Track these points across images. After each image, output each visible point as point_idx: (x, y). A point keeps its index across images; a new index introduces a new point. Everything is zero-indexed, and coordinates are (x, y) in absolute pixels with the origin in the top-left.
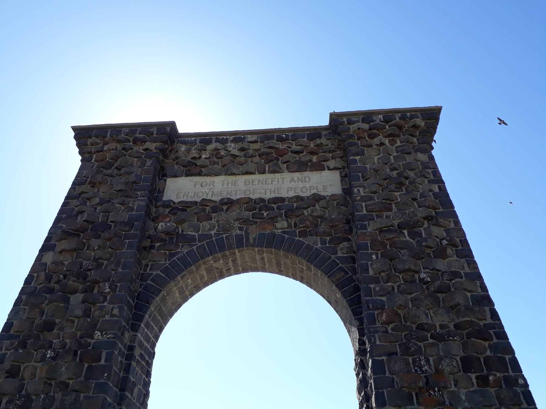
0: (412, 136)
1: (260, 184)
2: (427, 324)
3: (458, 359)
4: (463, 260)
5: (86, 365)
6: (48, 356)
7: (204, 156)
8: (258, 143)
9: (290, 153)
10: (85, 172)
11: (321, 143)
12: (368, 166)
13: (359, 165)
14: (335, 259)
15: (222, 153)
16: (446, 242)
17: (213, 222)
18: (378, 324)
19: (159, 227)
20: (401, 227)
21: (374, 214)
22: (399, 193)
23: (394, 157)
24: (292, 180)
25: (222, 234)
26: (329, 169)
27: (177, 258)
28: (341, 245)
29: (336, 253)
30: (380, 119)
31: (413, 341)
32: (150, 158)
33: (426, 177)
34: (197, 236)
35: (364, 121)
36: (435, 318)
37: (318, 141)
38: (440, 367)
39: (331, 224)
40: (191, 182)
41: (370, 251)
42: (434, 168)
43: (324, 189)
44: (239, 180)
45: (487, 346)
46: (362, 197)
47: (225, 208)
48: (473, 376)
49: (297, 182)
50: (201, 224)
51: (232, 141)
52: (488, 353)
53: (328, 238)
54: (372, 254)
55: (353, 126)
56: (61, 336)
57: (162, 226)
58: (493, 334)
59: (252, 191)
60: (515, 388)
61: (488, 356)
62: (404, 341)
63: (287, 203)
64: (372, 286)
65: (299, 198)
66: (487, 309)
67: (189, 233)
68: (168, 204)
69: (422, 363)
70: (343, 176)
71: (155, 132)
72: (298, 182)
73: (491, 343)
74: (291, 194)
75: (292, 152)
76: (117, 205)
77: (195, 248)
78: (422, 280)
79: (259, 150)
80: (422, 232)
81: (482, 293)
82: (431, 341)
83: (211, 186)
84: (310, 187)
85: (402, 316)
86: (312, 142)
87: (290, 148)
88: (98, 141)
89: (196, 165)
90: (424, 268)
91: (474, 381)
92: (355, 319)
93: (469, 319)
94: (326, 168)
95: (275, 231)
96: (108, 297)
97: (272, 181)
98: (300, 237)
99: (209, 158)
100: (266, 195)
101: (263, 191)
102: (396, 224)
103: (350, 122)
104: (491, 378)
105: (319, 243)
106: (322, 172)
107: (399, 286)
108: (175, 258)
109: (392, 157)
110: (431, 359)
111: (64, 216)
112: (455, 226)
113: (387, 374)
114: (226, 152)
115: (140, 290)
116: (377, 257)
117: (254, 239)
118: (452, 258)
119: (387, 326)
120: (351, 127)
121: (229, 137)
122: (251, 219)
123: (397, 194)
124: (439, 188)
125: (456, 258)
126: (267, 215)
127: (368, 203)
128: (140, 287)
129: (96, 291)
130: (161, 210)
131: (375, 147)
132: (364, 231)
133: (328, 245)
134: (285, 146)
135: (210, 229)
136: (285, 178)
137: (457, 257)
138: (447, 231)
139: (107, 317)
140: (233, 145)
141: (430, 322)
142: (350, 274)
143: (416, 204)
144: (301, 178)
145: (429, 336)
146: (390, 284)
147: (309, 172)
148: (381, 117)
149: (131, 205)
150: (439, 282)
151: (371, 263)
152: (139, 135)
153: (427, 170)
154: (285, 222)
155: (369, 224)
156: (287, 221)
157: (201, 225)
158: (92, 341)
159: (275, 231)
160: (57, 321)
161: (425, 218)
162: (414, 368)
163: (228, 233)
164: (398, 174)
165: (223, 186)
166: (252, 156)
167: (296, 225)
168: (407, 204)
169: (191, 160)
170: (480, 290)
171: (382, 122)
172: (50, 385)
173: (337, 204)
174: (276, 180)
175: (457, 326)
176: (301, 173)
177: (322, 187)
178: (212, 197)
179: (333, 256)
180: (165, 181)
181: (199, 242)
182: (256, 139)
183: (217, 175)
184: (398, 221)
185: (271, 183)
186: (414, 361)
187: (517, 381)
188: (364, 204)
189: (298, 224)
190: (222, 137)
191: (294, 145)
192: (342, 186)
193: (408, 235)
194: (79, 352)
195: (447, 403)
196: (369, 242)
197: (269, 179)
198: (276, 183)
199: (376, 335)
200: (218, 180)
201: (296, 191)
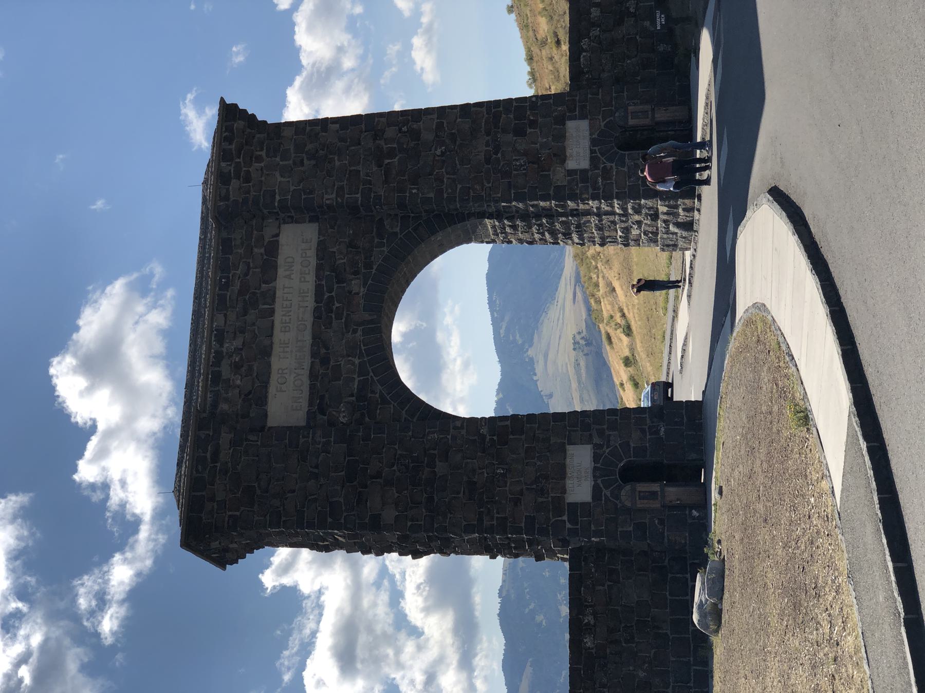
0: (254, 137)
1: (290, 314)
3: (515, 138)
4: (424, 118)
5: (511, 437)
7: (238, 382)
8: (228, 314)
9: (248, 277)
10: (256, 518)
11: (241, 238)
12: (292, 188)
13: (289, 197)
14: (402, 235)
15: (237, 360)
16: (406, 127)
17: (342, 363)
18: (483, 194)
19: (344, 420)
20: (380, 166)
21: (361, 187)
22: (336, 161)
23: (281, 161)
24: (289, 277)
25: (361, 350)
26: (278, 235)
27: (388, 394)
28: (388, 227)
29: (396, 234)
30: (227, 165)
31: (499, 168)
33: (318, 134)
34: (359, 379)
38: (522, 151)
40: (275, 397)
41: (408, 195)
42: (306, 124)
43: (307, 242)
44: (281, 340)
45: (505, 116)
46: (337, 196)
47: (323, 351)
48: (529, 130)
49: (293, 272)
50: (344, 376)
51: (222, 345)
52: (512, 116)
53: (376, 240)
54: (411, 193)
55: (231, 196)
56: (480, 471)
57: (344, 417)
58: (496, 110)
60: (539, 104)
61: (514, 117)
62: (499, 175)
63: (324, 283)
64: (445, 197)
65: (319, 268)
66: (473, 109)
67: (356, 386)
68: (310, 415)
69: (518, 164)
72: (293, 270)
73: (503, 112)
74: (311, 278)
75: (246, 274)
76: (320, 459)
77: (375, 379)
78: (443, 154)
79: (237, 312)
80: (389, 147)
82: (499, 155)
83: (284, 372)
84: (302, 257)
85: (476, 174)
87: (239, 278)
89: (250, 393)
90: (431, 151)
91: (532, 130)
92: (468, 221)
93: (483, 124)
94: (275, 239)
95: (361, 294)
96: (441, 436)
97: (286, 300)
100: (307, 307)
101: (301, 309)
102: (376, 168)
103: (226, 198)
104: (532, 118)
105: (382, 249)
106: (280, 244)
107: (447, 174)
108: (388, 397)
110: (514, 158)
111: (329, 520)
112: (385, 117)
113: (526, 191)
114: (234, 355)
116: (414, 188)
118: (421, 126)
119: (485, 187)
120: (232, 198)
121: (212, 350)
122: (343, 320)
123: (337, 163)
125: (421, 123)
126: (340, 303)
127: (346, 191)
129: (432, 452)
131: (263, 178)
132: (383, 197)
133: (385, 241)
134: (238, 284)
135: (353, 364)
136: (284, 285)
139: (464, 432)
141: (483, 154)
142: (421, 221)
143: (353, 148)
144: (287, 267)
145: (495, 156)
146: (445, 180)
147: (279, 257)
148: (223, 164)
149: (320, 446)
150: (447, 141)
151: (420, 194)
152: (208, 453)
153: (307, 130)
154: (353, 282)
155: (374, 192)
156: (352, 280)
157: (345, 376)
158: (488, 437)
159: (361, 294)
160: (465, 479)
161: (375, 139)
162: (521, 171)
163: (360, 344)
164: (309, 159)
165: (288, 358)
166: (245, 323)
167: (356, 273)
169: (241, 399)
170: (455, 111)
171: (231, 164)
172: (527, 463)
173: (332, 227)
175: (488, 134)
176: (278, 267)
177: (304, 244)
178: (303, 369)
179: (399, 237)
180: (270, 428)
182: (222, 315)
183: (270, 366)
184: (374, 166)
185: (290, 302)
186: (516, 170)
188: (347, 196)
189: (356, 269)
190: (211, 358)
191: (237, 272)
192: (305, 222)
193: (392, 159)
194: (498, 447)
195: (548, 151)
196: (396, 195)
197: (283, 304)
199: (492, 196)
200: (276, 363)
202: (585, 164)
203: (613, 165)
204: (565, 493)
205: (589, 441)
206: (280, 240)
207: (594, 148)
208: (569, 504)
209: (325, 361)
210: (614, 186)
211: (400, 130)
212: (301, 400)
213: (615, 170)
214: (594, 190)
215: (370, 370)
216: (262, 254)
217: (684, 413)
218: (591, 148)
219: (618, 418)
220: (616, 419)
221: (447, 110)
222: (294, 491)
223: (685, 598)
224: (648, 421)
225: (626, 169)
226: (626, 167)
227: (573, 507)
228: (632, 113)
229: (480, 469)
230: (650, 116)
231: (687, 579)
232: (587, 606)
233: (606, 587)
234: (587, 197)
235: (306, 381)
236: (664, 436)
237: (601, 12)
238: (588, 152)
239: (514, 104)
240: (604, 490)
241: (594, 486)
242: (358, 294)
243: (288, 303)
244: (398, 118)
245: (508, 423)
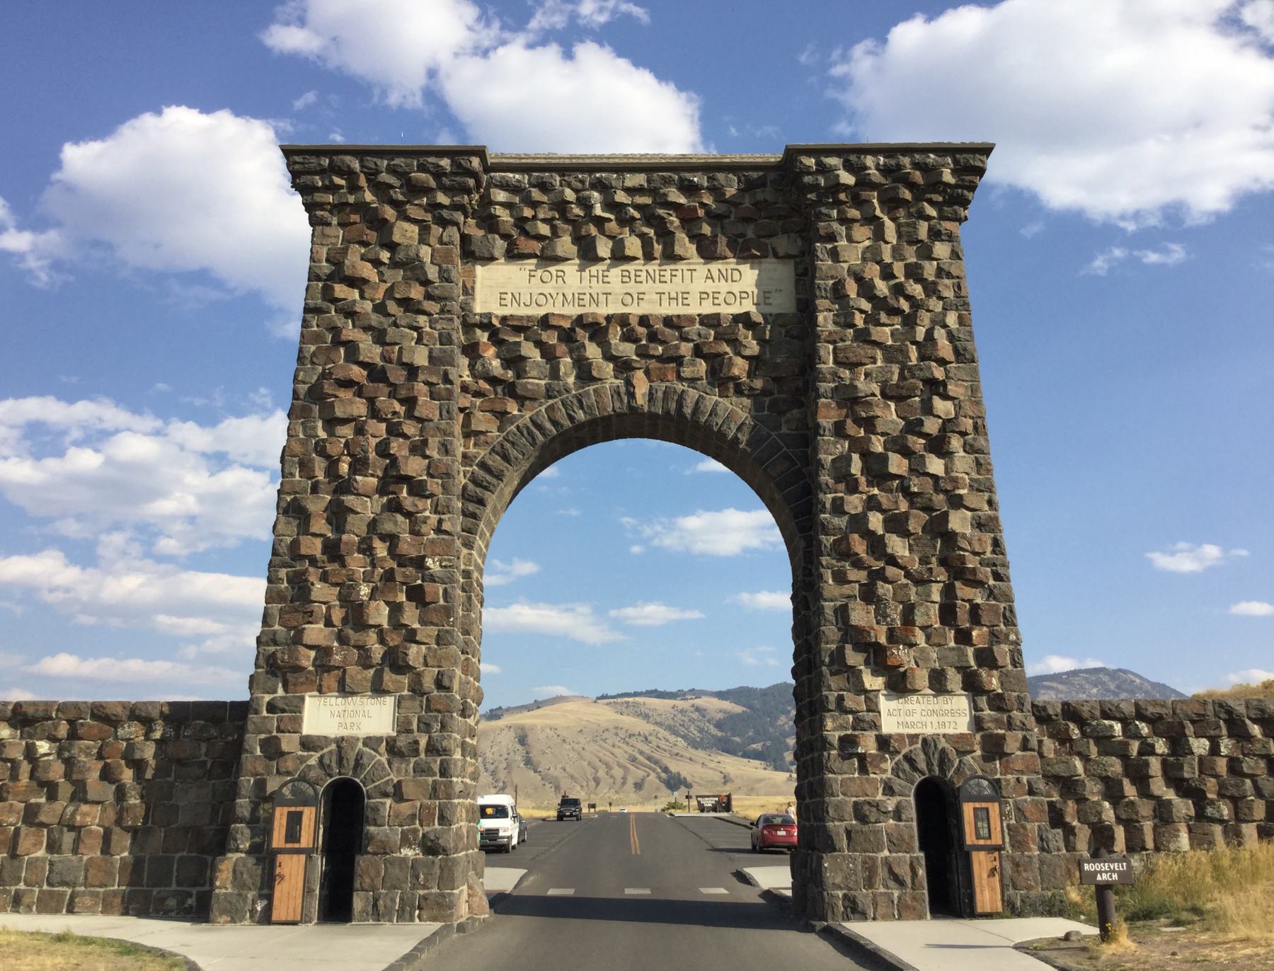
2: (902, 557)
6: (362, 593)
7: (541, 216)
11: (766, 201)
26: (776, 255)
27: (518, 427)
28: (788, 415)
29: (779, 427)
32: (444, 223)
35: (849, 167)
36: (915, 548)
37: (760, 195)
39: (773, 375)
49: (717, 281)
53: (767, 400)
59: (635, 298)
70: (800, 271)
71: (448, 169)
74: (707, 309)
76: (407, 330)
81: (990, 512)
82: (904, 581)
86: (747, 196)
88: (343, 182)
94: (771, 251)
97: (672, 275)
98: (720, 396)
99: (553, 219)
104: (974, 633)
109: (889, 246)
115: (464, 481)
117: (643, 395)
122: (635, 357)
124: (960, 318)
125: (962, 453)
128: (465, 476)
130: (478, 332)
133: (766, 413)
137: (965, 451)
138: (958, 407)
140: (596, 194)
151: (830, 458)
153: (946, 281)
162: (876, 617)
168: (901, 351)
170: (986, 507)
174: (679, 273)
179: (773, 433)
181: (550, 397)
187: (1007, 636)
198: (678, 280)
200: (570, 269)
201: (716, 302)
202: (889, 726)
203: (889, 775)
204: (320, 691)
205: (403, 726)
206: (768, 260)
207: (920, 741)
208: (302, 699)
209: (567, 336)
210: (847, 776)
211: (949, 420)
212: (515, 304)
213: (878, 777)
214: (841, 739)
215: (556, 400)
216: (743, 235)
217: (433, 891)
218: (921, 737)
219: (438, 778)
220: (434, 774)
221: (986, 496)
222: (362, 297)
223: (174, 879)
224: (427, 829)
225: (880, 797)
226: (884, 798)
227: (297, 708)
228: (987, 809)
229: (373, 560)
230: (982, 842)
231: (203, 885)
232: (177, 729)
233: (203, 758)
234: (828, 728)
235: (541, 312)
236: (398, 855)
237: (1201, 758)
238: (912, 731)
239: (1002, 605)
240: (318, 755)
241: (325, 737)
242: (680, 378)
243: (668, 278)
244: (972, 418)
245: (442, 602)
